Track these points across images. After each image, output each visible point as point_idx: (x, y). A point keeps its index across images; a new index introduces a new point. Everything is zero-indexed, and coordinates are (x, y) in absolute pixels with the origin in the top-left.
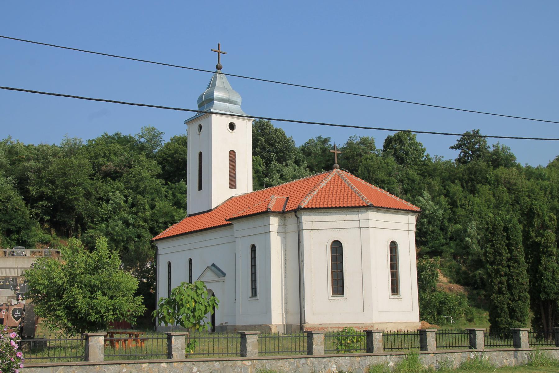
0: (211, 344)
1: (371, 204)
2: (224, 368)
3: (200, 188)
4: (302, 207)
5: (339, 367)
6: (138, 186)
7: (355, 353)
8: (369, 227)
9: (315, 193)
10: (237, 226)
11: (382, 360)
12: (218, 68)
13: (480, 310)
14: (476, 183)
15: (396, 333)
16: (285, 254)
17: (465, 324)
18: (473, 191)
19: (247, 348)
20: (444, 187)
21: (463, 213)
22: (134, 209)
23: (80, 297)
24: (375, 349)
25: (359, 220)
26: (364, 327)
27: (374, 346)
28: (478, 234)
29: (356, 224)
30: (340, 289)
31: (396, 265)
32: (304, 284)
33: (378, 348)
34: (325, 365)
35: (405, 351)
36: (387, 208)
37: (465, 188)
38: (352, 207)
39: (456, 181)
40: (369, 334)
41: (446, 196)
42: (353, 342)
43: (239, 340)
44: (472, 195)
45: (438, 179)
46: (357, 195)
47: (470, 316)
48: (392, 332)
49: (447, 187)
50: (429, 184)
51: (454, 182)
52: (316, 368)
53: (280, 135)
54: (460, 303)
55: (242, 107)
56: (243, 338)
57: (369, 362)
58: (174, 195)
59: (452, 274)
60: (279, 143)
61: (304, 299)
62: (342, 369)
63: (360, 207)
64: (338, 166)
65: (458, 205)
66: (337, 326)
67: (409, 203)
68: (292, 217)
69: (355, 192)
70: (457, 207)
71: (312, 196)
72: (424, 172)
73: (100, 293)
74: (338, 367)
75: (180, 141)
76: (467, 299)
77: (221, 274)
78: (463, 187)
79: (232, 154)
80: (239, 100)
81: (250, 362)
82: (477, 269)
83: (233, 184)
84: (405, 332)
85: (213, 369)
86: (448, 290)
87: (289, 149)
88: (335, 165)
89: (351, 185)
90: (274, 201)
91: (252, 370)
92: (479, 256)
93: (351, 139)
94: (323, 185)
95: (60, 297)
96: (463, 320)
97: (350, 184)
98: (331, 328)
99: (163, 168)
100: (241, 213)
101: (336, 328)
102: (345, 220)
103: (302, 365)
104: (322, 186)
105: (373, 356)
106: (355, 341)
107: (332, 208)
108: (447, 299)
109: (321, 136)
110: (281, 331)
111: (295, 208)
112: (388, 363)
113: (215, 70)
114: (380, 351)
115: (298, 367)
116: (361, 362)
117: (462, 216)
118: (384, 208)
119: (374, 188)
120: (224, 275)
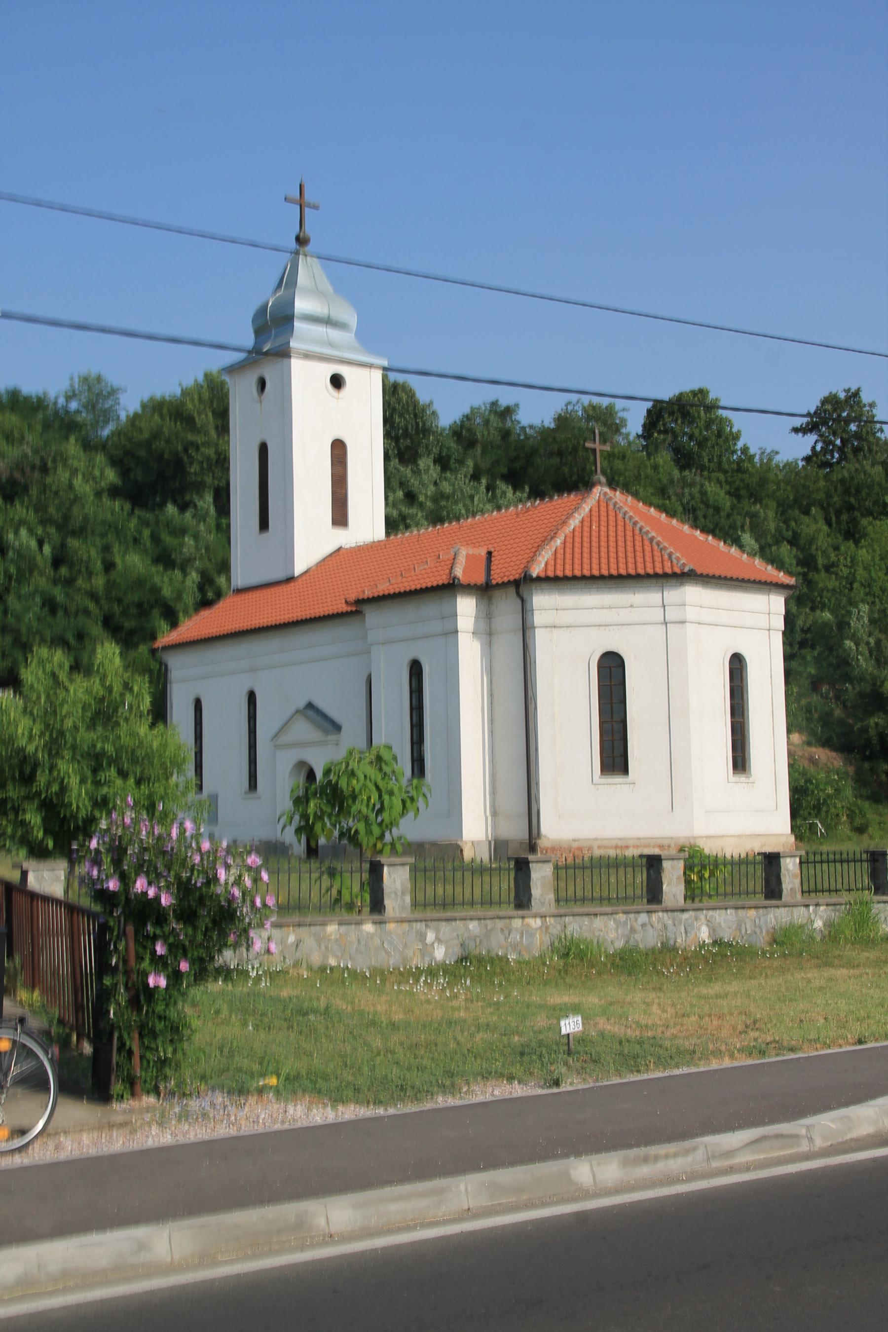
0: (495, 880)
1: (691, 571)
2: (488, 934)
3: (264, 525)
4: (534, 575)
5: (714, 930)
6: (66, 518)
7: (706, 902)
8: (684, 622)
9: (558, 542)
10: (373, 617)
11: (800, 915)
12: (301, 241)
13: (881, 808)
14: (859, 515)
15: (751, 858)
16: (491, 683)
17: (850, 839)
18: (852, 534)
19: (533, 892)
20: (786, 522)
21: (832, 583)
22: (64, 571)
23: (74, 781)
24: (785, 893)
25: (769, 614)
26: (673, 845)
27: (784, 886)
28: (870, 635)
29: (658, 614)
30: (619, 761)
31: (743, 707)
32: (537, 750)
33: (791, 889)
34: (687, 927)
35: (845, 897)
36: (725, 578)
37: (834, 525)
38: (648, 576)
39: (813, 510)
40: (653, 863)
41: (791, 543)
42: (701, 878)
43: (366, 876)
44: (851, 544)
45: (773, 504)
46: (655, 547)
47: (858, 822)
48: (743, 855)
49: (793, 524)
50: (754, 516)
51: (806, 512)
52: (668, 934)
53: (404, 397)
54: (838, 791)
55: (358, 335)
56: (521, 869)
57: (773, 920)
58: (155, 539)
59: (812, 726)
60: (401, 415)
61: (537, 784)
62: (722, 935)
63: (665, 576)
64: (603, 479)
65: (820, 566)
66: (614, 843)
67: (769, 567)
68: (506, 598)
69: (651, 540)
70: (817, 570)
71: (554, 549)
72: (738, 489)
73: (113, 772)
74: (713, 930)
75: (165, 411)
76: (850, 782)
77: (329, 726)
78: (829, 523)
79: (339, 449)
80: (351, 317)
81: (539, 921)
82: (871, 714)
83: (340, 517)
84: (742, 857)
85: (466, 935)
86: (807, 762)
87: (426, 431)
88: (595, 478)
89: (639, 526)
90: (462, 560)
91: (543, 937)
92: (874, 684)
93: (570, 408)
94: (574, 522)
95: (28, 779)
96: (844, 828)
97: (635, 523)
98: (599, 847)
99: (124, 473)
100: (384, 588)
101: (611, 848)
102: (632, 606)
103: (640, 928)
104: (572, 527)
105: (781, 906)
106: (707, 875)
107: (602, 577)
108: (812, 783)
109: (497, 401)
110: (484, 855)
111: (517, 576)
112: (812, 922)
113: (293, 245)
114: (796, 897)
115: (633, 930)
116: (757, 921)
117: (828, 590)
118: (719, 578)
119: (688, 532)
120: (337, 728)
